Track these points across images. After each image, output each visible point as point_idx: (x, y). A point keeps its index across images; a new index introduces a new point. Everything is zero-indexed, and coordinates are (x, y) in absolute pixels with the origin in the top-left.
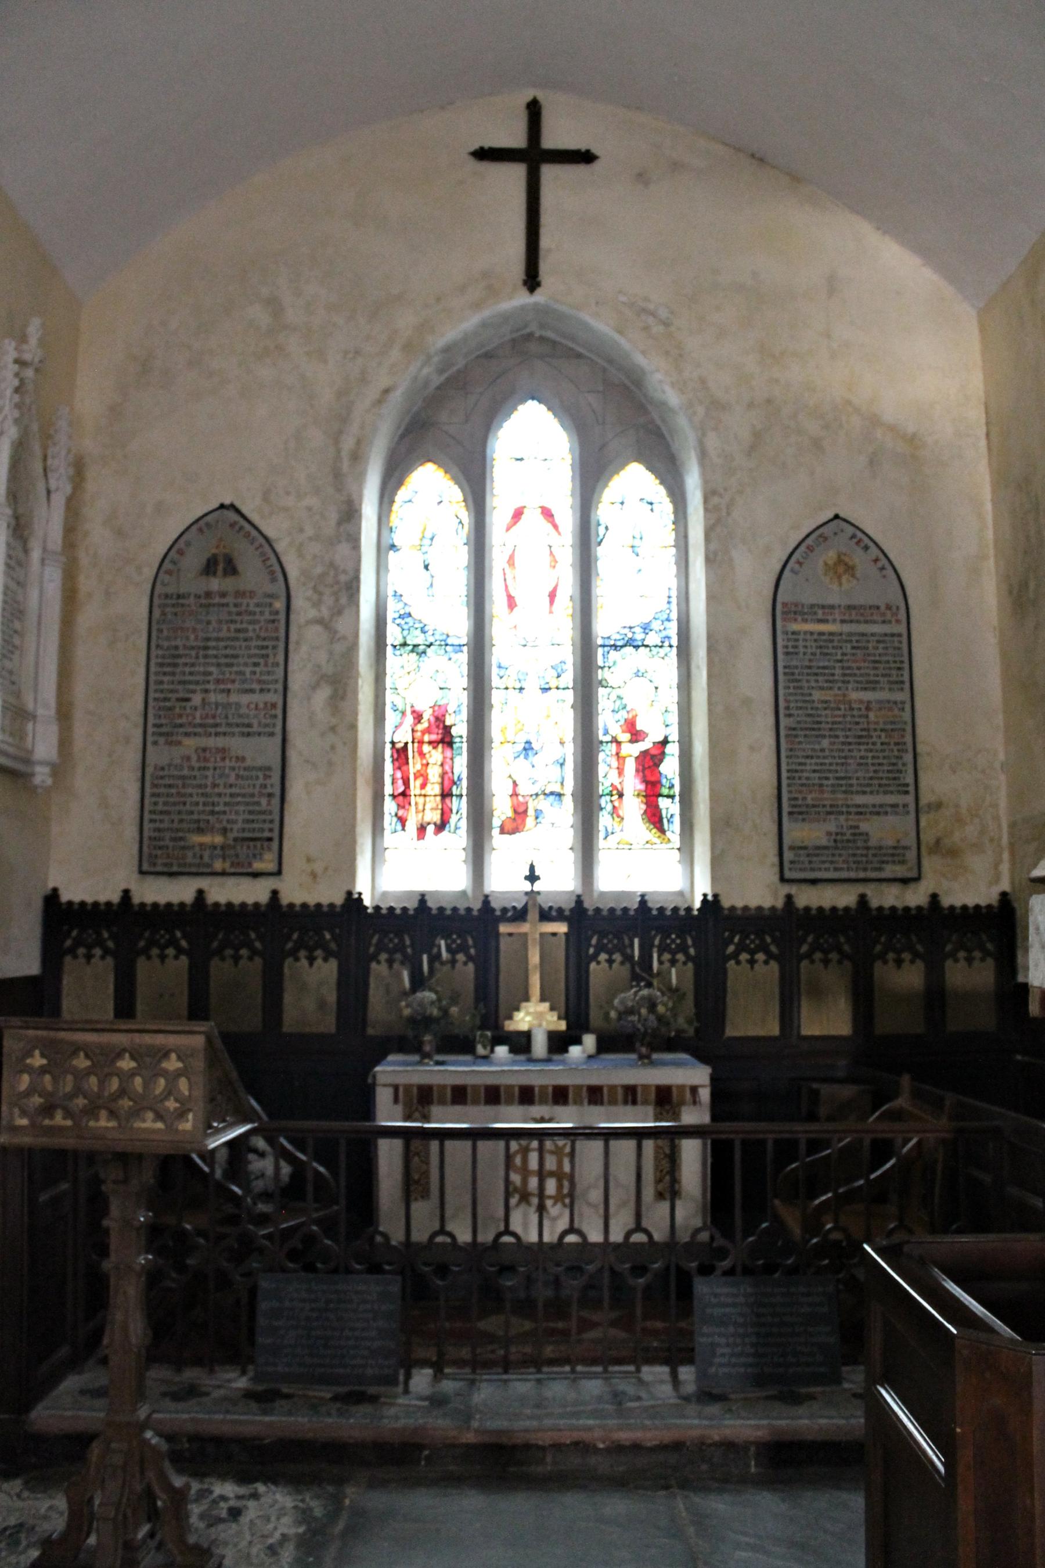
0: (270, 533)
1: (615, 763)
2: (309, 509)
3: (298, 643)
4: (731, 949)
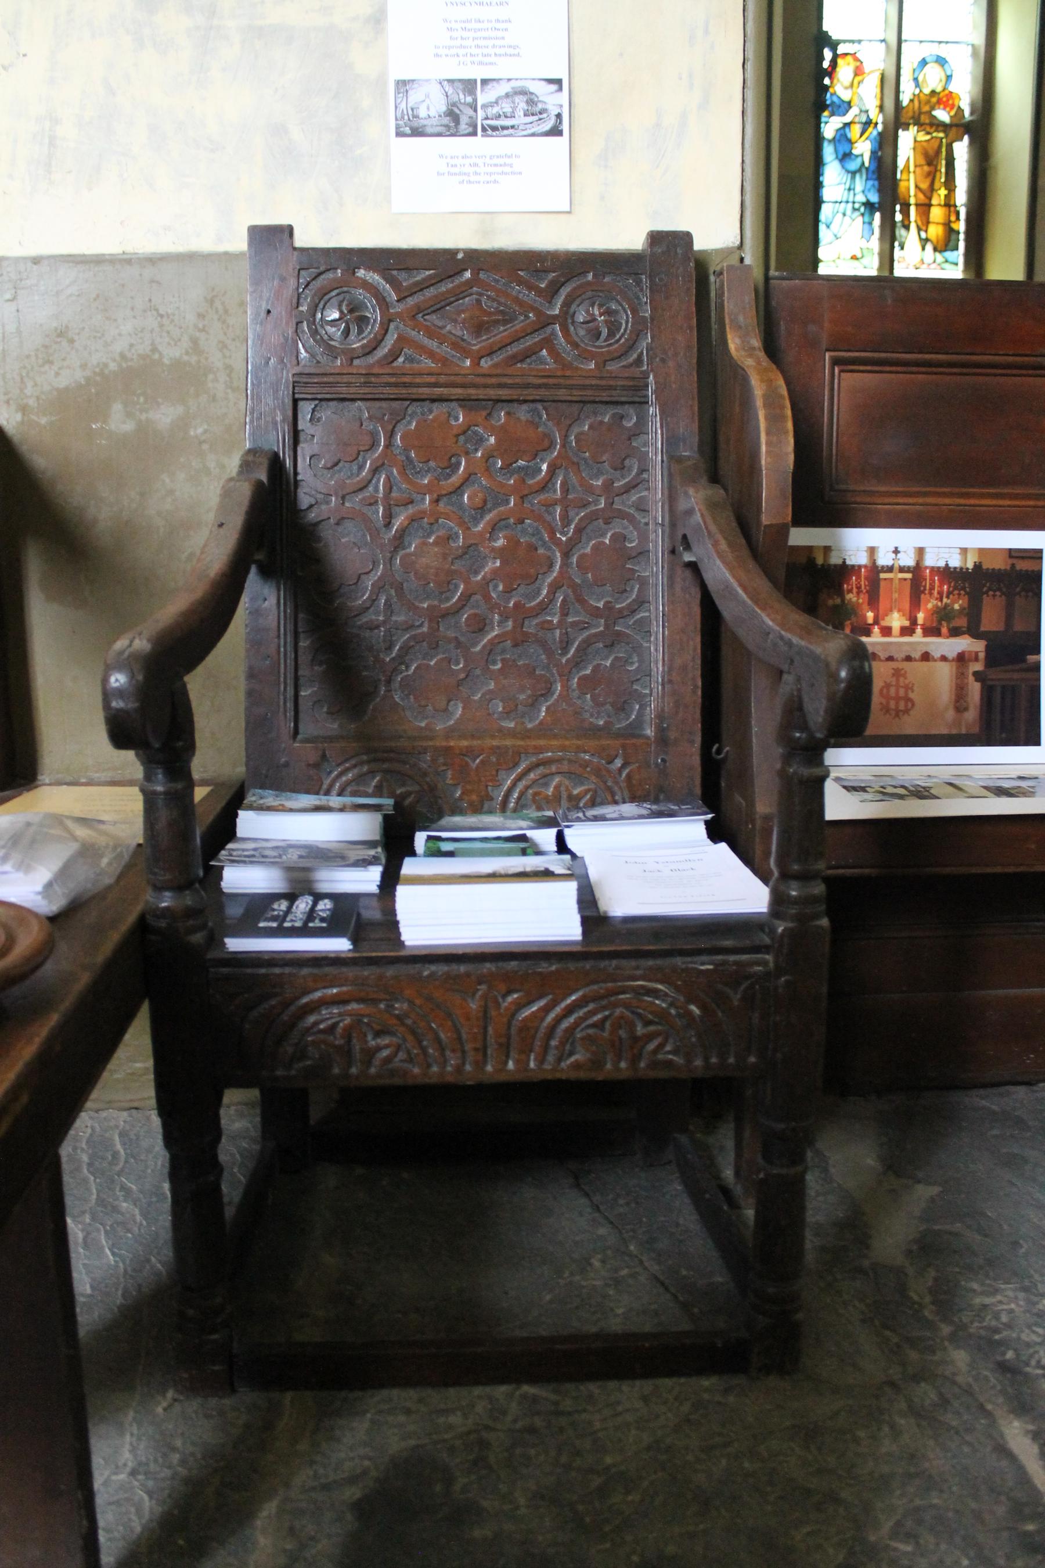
4: (985, 589)
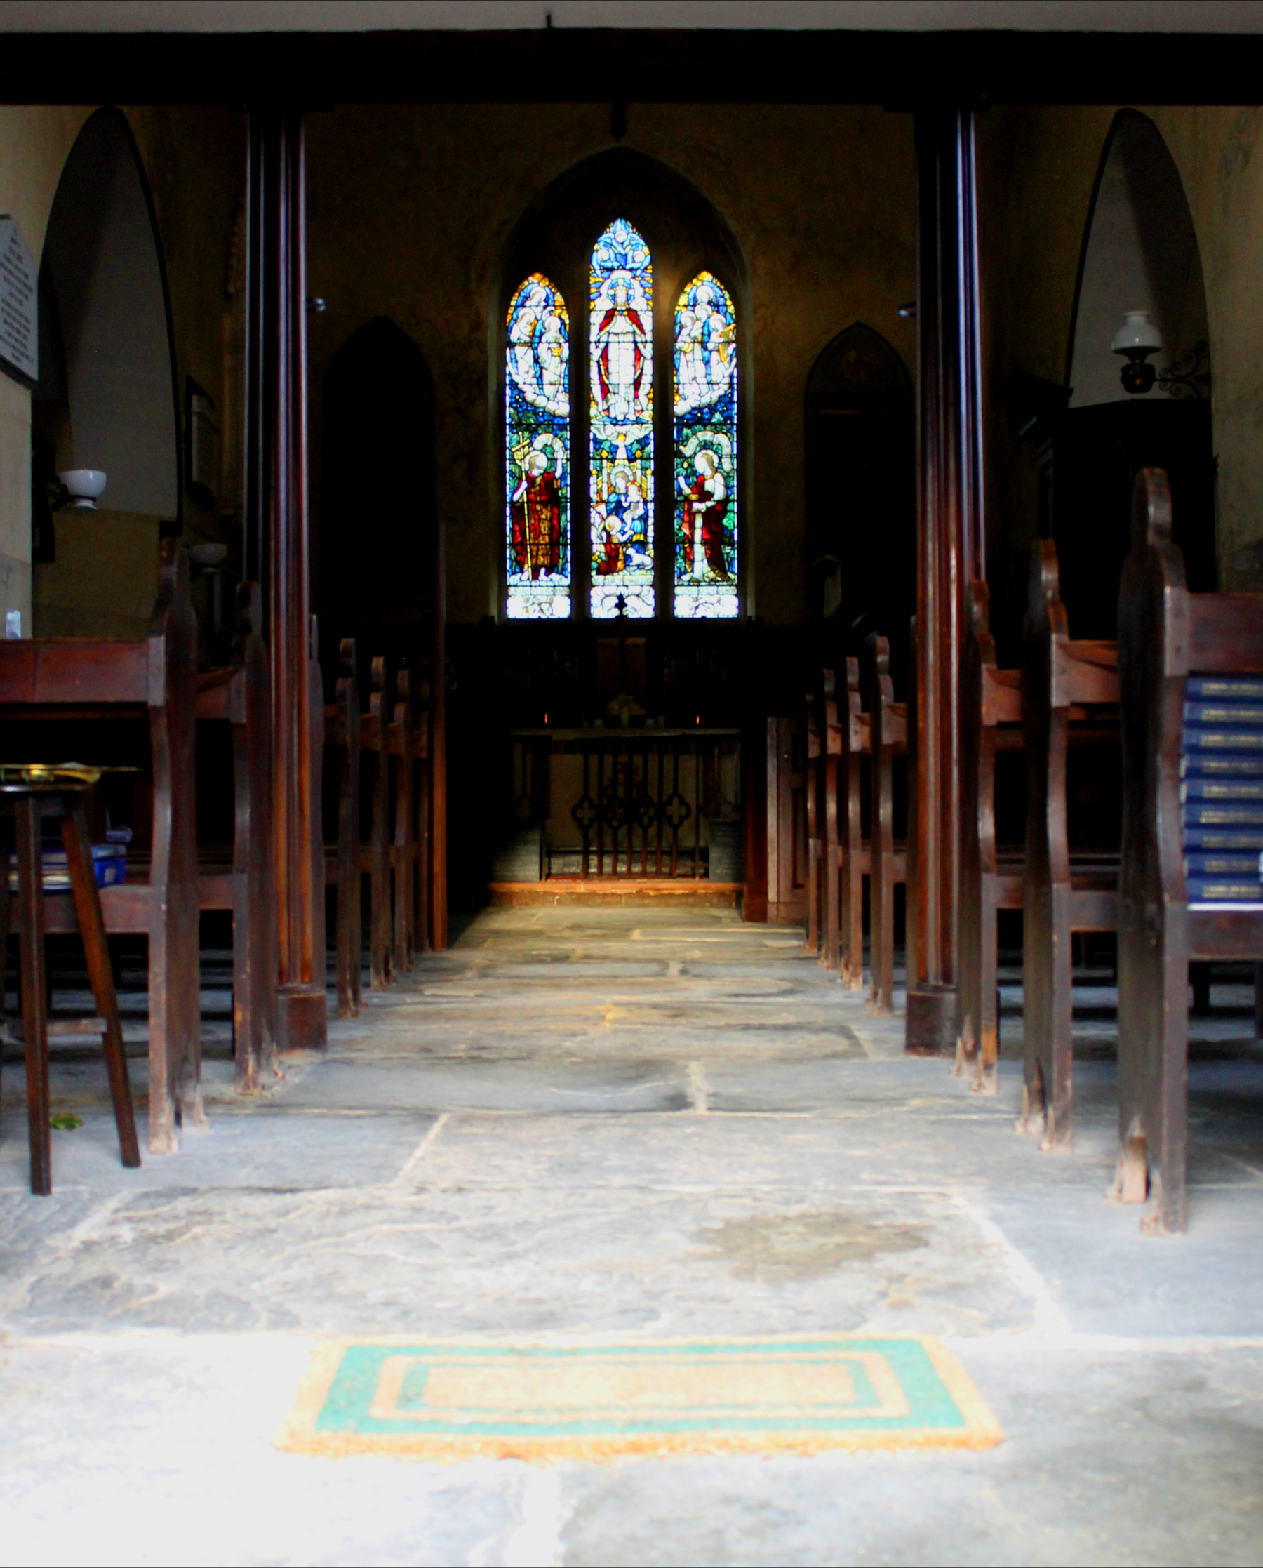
1: (686, 518)
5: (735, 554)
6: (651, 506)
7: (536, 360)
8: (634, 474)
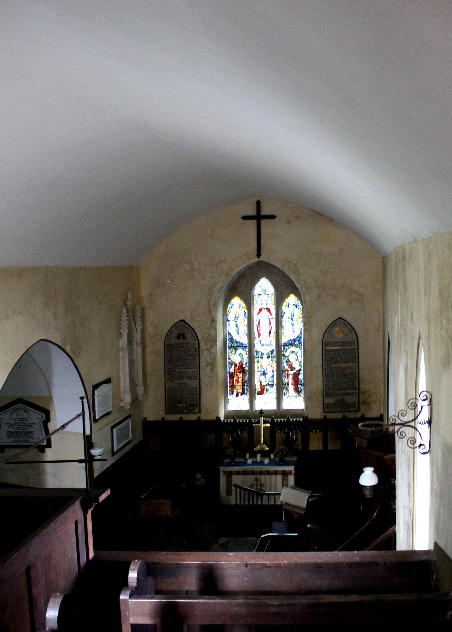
0: (193, 326)
1: (287, 376)
2: (203, 320)
3: (202, 355)
4: (311, 429)
5: (302, 388)
6: (275, 373)
7: (237, 325)
8: (269, 362)
